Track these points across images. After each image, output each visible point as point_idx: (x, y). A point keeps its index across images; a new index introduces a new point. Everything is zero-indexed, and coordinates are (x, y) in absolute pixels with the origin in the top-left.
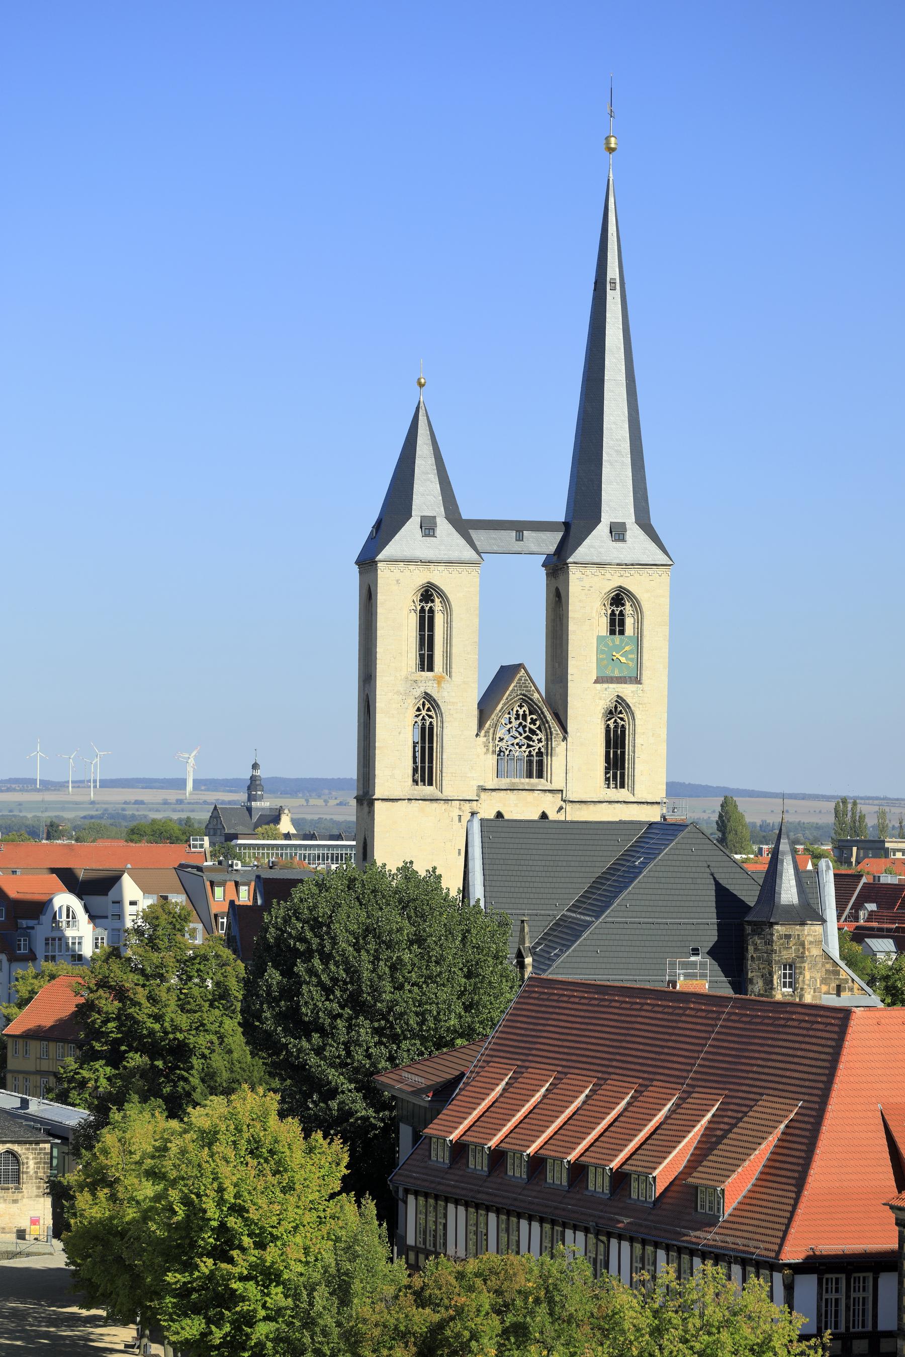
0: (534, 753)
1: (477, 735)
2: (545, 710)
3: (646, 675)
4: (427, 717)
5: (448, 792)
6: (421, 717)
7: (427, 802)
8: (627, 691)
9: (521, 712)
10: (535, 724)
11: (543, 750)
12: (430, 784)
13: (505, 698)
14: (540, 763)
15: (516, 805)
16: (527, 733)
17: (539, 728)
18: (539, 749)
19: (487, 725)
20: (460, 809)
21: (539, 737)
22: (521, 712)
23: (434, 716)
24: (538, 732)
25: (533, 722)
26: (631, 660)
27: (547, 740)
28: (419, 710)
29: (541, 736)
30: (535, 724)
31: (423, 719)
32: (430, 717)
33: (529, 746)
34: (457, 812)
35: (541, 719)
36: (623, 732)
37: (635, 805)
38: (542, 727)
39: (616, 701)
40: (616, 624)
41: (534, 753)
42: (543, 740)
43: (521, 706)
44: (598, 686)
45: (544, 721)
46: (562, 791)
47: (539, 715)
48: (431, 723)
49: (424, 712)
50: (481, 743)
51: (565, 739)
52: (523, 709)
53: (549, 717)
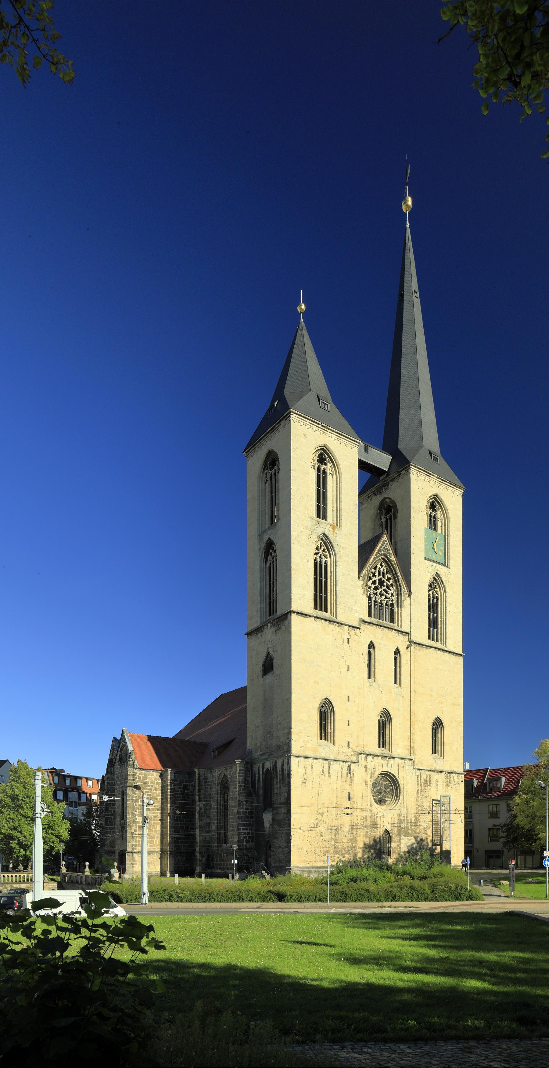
0: (389, 603)
1: (359, 577)
2: (398, 570)
3: (452, 563)
4: (323, 556)
5: (340, 618)
6: (319, 555)
7: (327, 623)
8: (442, 570)
9: (381, 570)
10: (389, 582)
11: (394, 602)
12: (326, 611)
13: (375, 554)
14: (392, 611)
15: (382, 639)
16: (385, 587)
17: (392, 585)
18: (392, 601)
19: (364, 572)
20: (349, 633)
21: (392, 592)
22: (381, 570)
23: (328, 556)
24: (391, 588)
25: (389, 579)
26: (441, 551)
27: (398, 595)
28: (317, 549)
29: (393, 591)
30: (389, 582)
31: (320, 557)
32: (325, 557)
33: (386, 598)
34: (346, 636)
35: (394, 578)
36: (437, 602)
37: (447, 654)
38: (394, 585)
39: (434, 578)
40: (433, 523)
41: (389, 603)
42: (394, 595)
43: (381, 565)
44: (427, 562)
45: (396, 581)
46: (408, 633)
47: (393, 575)
48: (325, 563)
49: (321, 552)
50: (360, 585)
51: (409, 596)
52: (383, 568)
53: (400, 577)
